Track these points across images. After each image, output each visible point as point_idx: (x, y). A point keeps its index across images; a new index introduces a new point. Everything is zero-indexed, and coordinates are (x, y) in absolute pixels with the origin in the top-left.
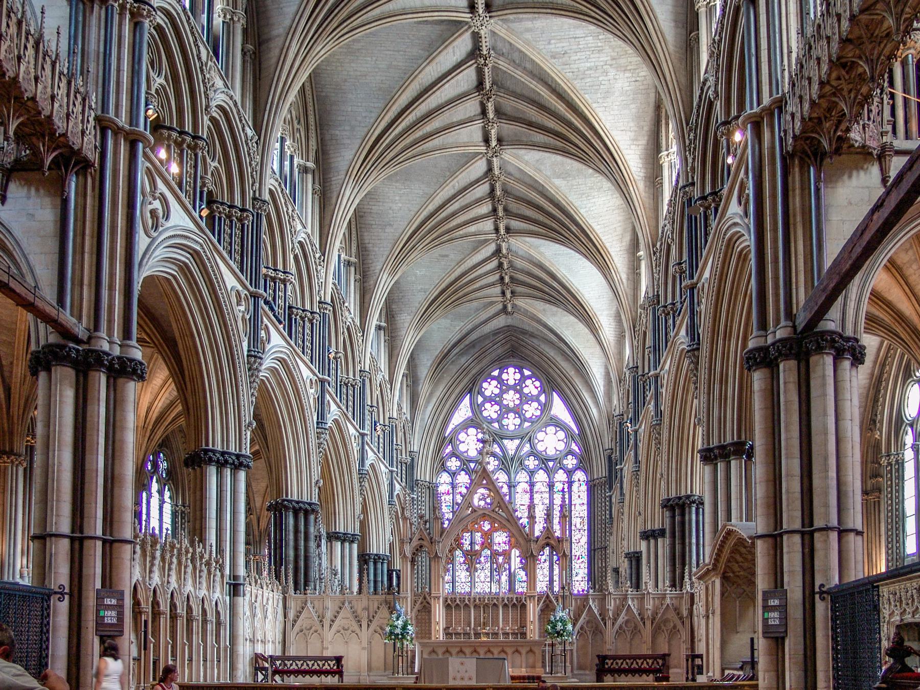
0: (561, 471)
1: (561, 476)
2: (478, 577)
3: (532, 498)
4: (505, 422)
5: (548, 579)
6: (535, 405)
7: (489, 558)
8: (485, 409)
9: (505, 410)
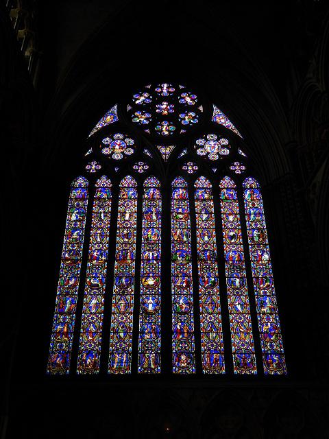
0: (227, 179)
1: (226, 182)
2: (118, 306)
3: (192, 207)
4: (158, 128)
5: (218, 310)
6: (193, 114)
8: (137, 117)
9: (159, 118)
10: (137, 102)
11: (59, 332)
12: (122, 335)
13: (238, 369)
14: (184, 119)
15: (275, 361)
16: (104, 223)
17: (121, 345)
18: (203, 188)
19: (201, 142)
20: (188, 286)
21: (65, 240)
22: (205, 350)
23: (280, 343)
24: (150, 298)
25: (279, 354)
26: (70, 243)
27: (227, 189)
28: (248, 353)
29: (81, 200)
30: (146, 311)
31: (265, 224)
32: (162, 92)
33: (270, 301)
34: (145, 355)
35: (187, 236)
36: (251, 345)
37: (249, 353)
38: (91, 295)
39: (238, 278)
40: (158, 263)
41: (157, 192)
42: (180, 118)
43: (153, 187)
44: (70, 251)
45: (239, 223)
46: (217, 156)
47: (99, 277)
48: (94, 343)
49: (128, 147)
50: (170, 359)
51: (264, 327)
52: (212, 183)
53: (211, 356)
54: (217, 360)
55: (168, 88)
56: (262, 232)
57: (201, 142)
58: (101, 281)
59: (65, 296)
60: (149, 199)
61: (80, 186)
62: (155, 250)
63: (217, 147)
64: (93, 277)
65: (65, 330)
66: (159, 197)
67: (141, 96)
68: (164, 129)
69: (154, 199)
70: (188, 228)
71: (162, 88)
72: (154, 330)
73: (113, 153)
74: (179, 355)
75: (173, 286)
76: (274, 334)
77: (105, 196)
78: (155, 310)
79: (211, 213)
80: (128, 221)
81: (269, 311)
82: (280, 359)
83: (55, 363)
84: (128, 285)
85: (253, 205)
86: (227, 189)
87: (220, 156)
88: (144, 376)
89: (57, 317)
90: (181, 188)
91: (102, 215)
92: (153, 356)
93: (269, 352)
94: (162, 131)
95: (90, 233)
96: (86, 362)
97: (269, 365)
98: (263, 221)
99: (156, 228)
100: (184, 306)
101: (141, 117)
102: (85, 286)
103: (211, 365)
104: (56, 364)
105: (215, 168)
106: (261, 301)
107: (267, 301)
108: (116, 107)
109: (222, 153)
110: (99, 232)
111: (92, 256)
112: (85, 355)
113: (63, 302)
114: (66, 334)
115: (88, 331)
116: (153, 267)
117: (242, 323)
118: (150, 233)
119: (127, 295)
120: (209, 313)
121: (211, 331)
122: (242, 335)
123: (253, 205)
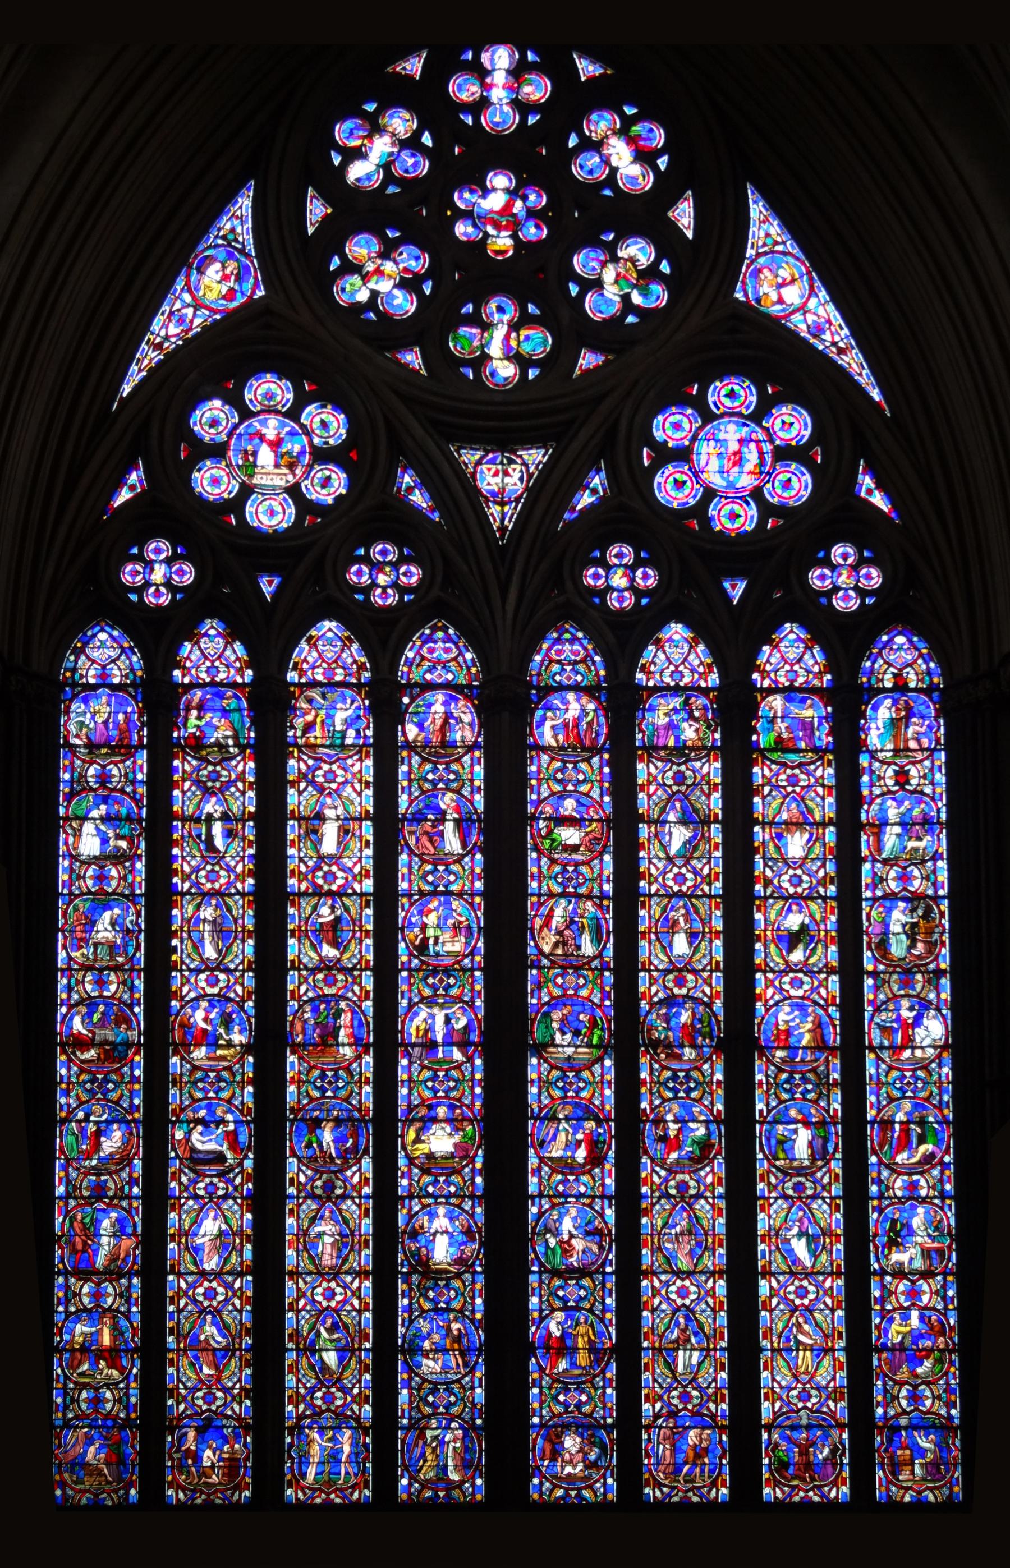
0: (791, 634)
2: (307, 1242)
7: (368, 1139)
8: (351, 268)
10: (357, 171)
11: (84, 1349)
12: (331, 1358)
13: (777, 1484)
14: (597, 284)
15: (922, 1452)
16: (229, 870)
17: (330, 1399)
18: (676, 690)
19: (677, 426)
20: (595, 1159)
21: (62, 955)
22: (657, 1416)
23: (949, 1390)
24: (441, 1210)
25: (942, 1428)
26: (86, 968)
27: (790, 692)
28: (819, 1426)
29: (114, 750)
30: (423, 1265)
31: (943, 876)
32: (483, 104)
33: (928, 1223)
34: (422, 1435)
35: (598, 936)
36: (836, 1395)
37: (826, 1424)
38: (196, 1197)
39: (807, 1124)
40: (470, 1059)
41: (465, 713)
42: (579, 280)
43: (446, 686)
44: (90, 1003)
45: (830, 867)
46: (753, 511)
47: (223, 1121)
48: (225, 1390)
49: (321, 455)
50: (523, 1447)
51: (895, 1327)
52: (720, 659)
53: (678, 1433)
54: (700, 1453)
55: (518, 72)
56: (927, 915)
57: (677, 426)
58: (232, 1138)
59: (89, 1201)
60: (423, 749)
61: (104, 680)
62: (459, 999)
63: (752, 456)
64: (198, 1121)
65: (106, 1340)
66: (469, 736)
67: (375, 128)
68: (495, 349)
69: (447, 745)
70: (603, 896)
71: (482, 74)
72: (458, 1339)
73: (247, 491)
74: (554, 1432)
75: (533, 1161)
76: (928, 1352)
77: (221, 732)
78: (460, 1261)
79: (707, 821)
80: (336, 859)
81: (918, 1264)
82: (941, 1446)
83: (79, 1464)
84: (349, 1156)
85: (902, 778)
86: (790, 692)
87: (766, 509)
88: (416, 1507)
89: (67, 1287)
90: (576, 688)
91: (217, 828)
92: (453, 1437)
93: (903, 1421)
94: (486, 358)
95: (169, 919)
96: (197, 1458)
97: (895, 1467)
98: (936, 857)
99: (460, 894)
100: (578, 1244)
101: (379, 272)
102: (164, 1162)
103: (678, 1470)
104: (85, 1465)
105: (734, 574)
106: (894, 1221)
107: (917, 1222)
108: (245, 203)
109: (775, 493)
110: (208, 913)
111: (186, 1026)
112: (192, 1434)
113: (84, 1228)
114: (112, 1356)
115: (198, 1347)
116: (448, 1078)
117: (809, 1310)
118: (432, 919)
119: (344, 1197)
120: (678, 1274)
121: (682, 1343)
122: (805, 1359)
123: (902, 778)
